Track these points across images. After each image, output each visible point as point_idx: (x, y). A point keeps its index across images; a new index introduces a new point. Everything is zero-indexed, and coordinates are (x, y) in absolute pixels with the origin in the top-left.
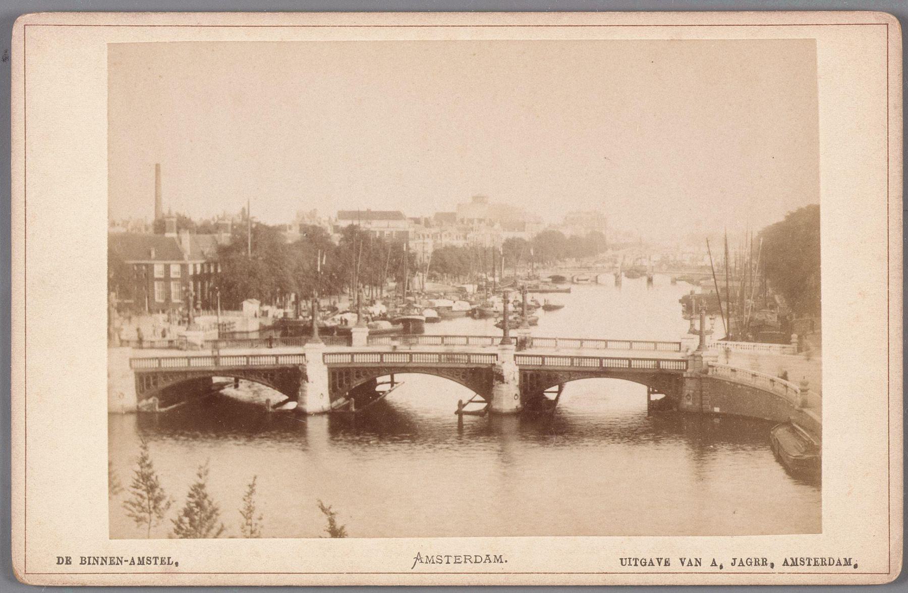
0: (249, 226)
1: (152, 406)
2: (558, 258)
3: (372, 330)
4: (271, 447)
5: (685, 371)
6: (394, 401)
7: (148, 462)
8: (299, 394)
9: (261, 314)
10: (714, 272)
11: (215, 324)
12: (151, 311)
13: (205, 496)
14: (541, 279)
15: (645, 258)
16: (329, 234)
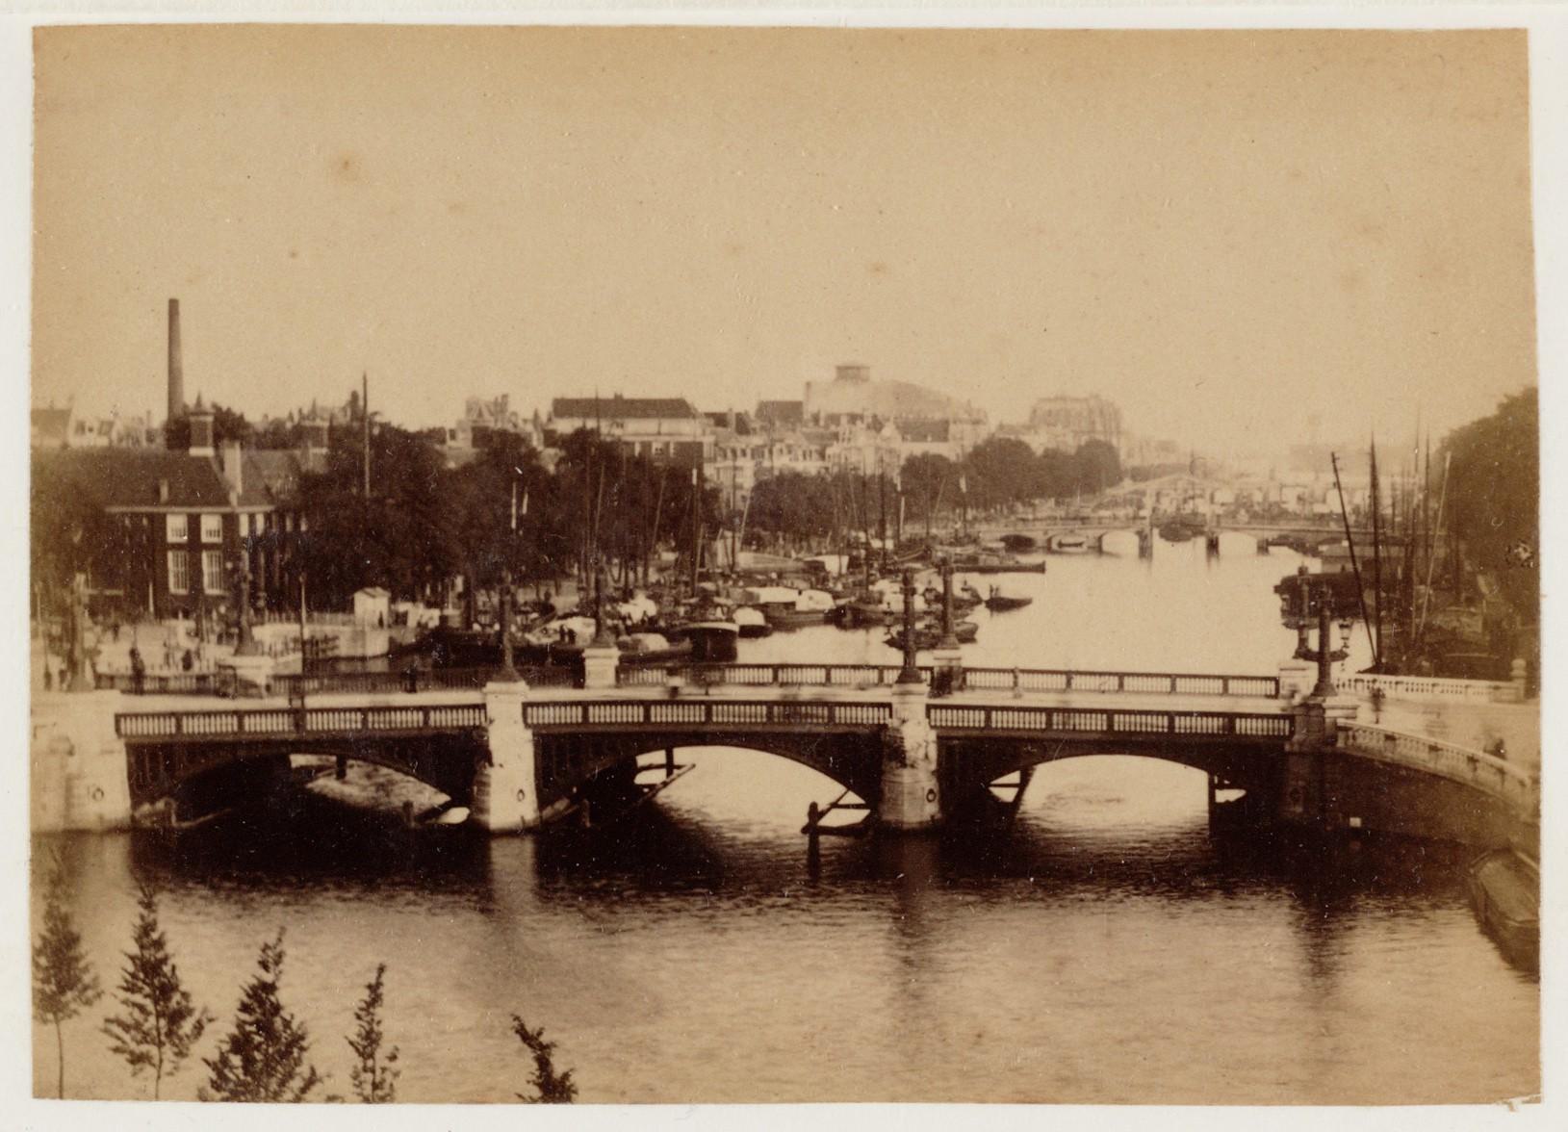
0: (367, 431)
1: (164, 816)
2: (1018, 498)
3: (626, 653)
4: (414, 903)
6: (674, 806)
7: (155, 936)
8: (472, 791)
9: (391, 621)
10: (1347, 527)
11: (295, 640)
12: (160, 615)
13: (277, 1008)
14: (983, 544)
15: (1201, 496)
16: (534, 449)
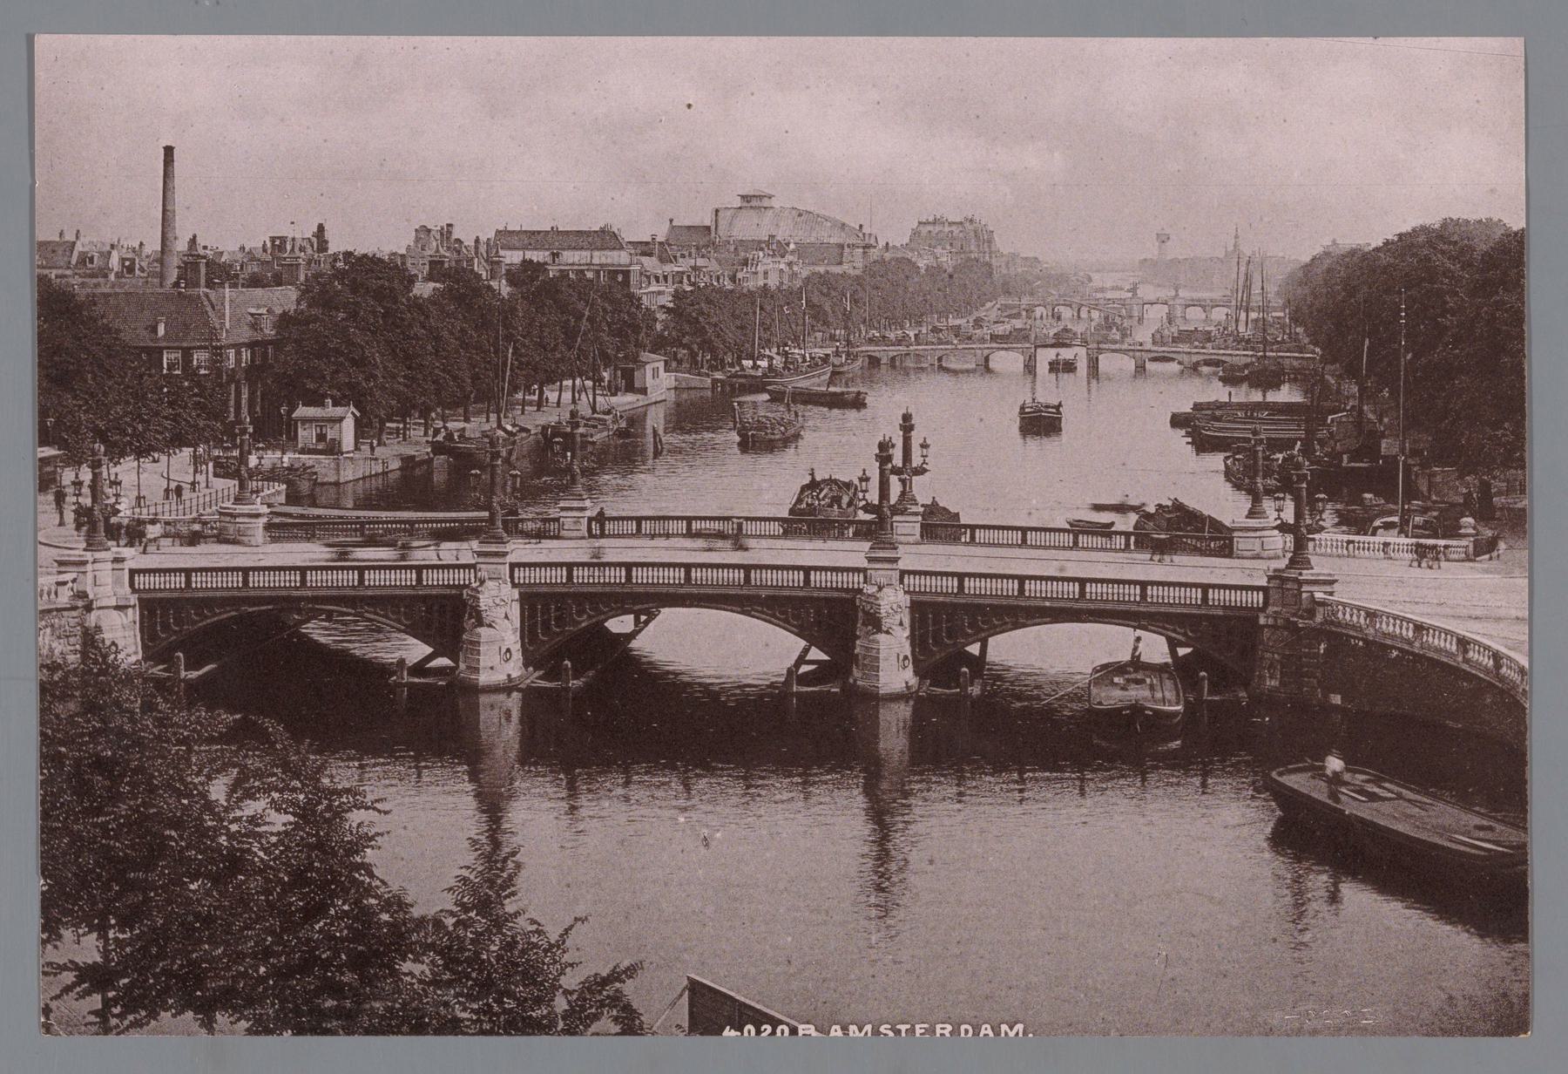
5: (1263, 610)
